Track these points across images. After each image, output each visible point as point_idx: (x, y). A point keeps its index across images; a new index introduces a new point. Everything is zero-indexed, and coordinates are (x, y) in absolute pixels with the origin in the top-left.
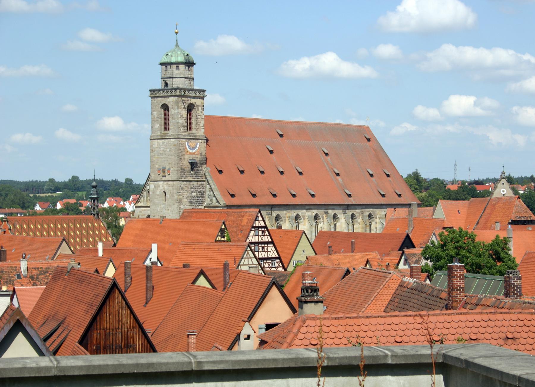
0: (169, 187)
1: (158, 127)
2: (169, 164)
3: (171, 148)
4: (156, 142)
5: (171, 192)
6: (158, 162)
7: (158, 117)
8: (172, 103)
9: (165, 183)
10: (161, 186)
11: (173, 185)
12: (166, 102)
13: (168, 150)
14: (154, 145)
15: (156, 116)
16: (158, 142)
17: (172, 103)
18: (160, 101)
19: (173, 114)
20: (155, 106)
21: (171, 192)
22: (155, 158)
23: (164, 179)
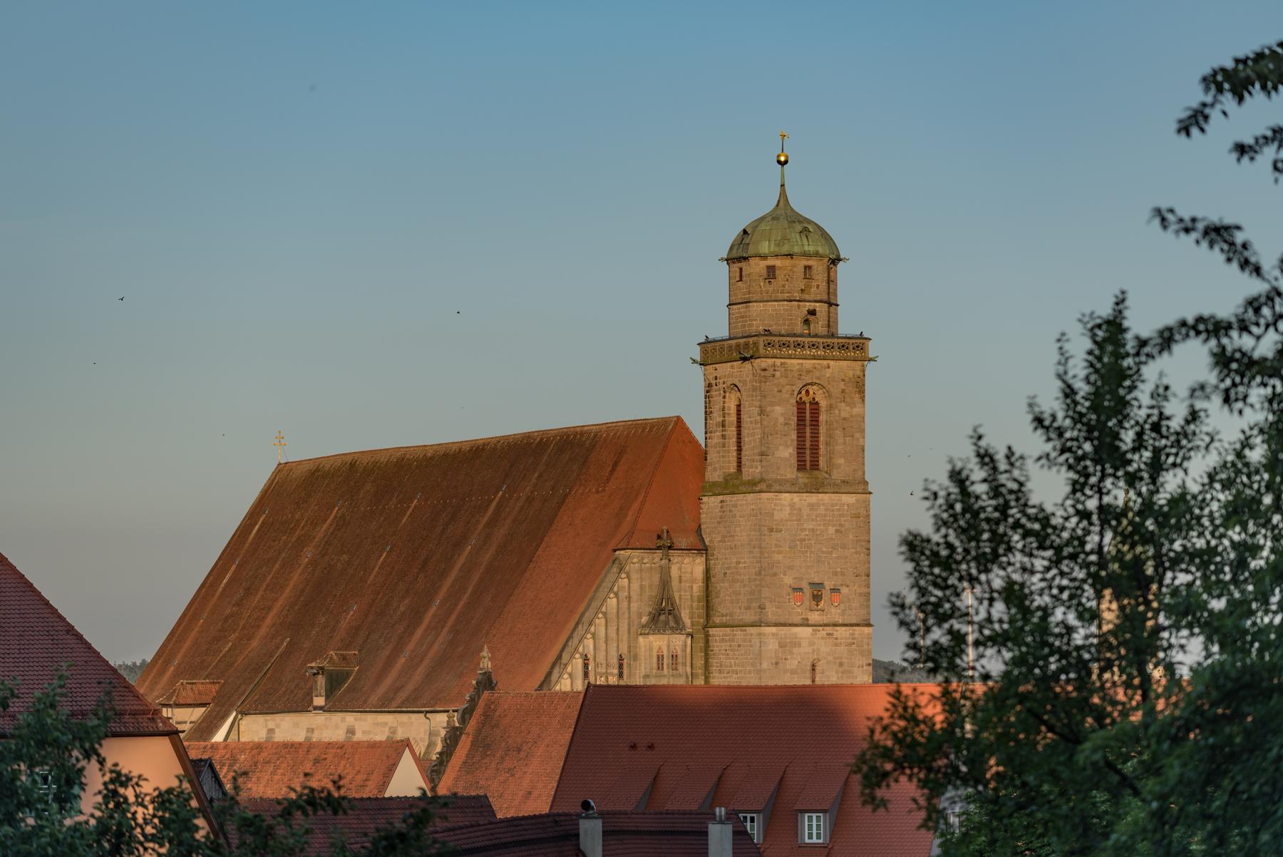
0: (836, 645)
1: (786, 454)
2: (836, 574)
3: (841, 525)
4: (786, 503)
5: (841, 665)
6: (790, 568)
7: (786, 424)
8: (842, 386)
9: (823, 632)
10: (805, 643)
11: (851, 641)
12: (818, 378)
13: (831, 530)
14: (775, 513)
15: (781, 420)
16: (792, 505)
17: (842, 386)
18: (796, 375)
19: (844, 419)
20: (776, 389)
21: (841, 665)
22: (779, 553)
23: (815, 617)
